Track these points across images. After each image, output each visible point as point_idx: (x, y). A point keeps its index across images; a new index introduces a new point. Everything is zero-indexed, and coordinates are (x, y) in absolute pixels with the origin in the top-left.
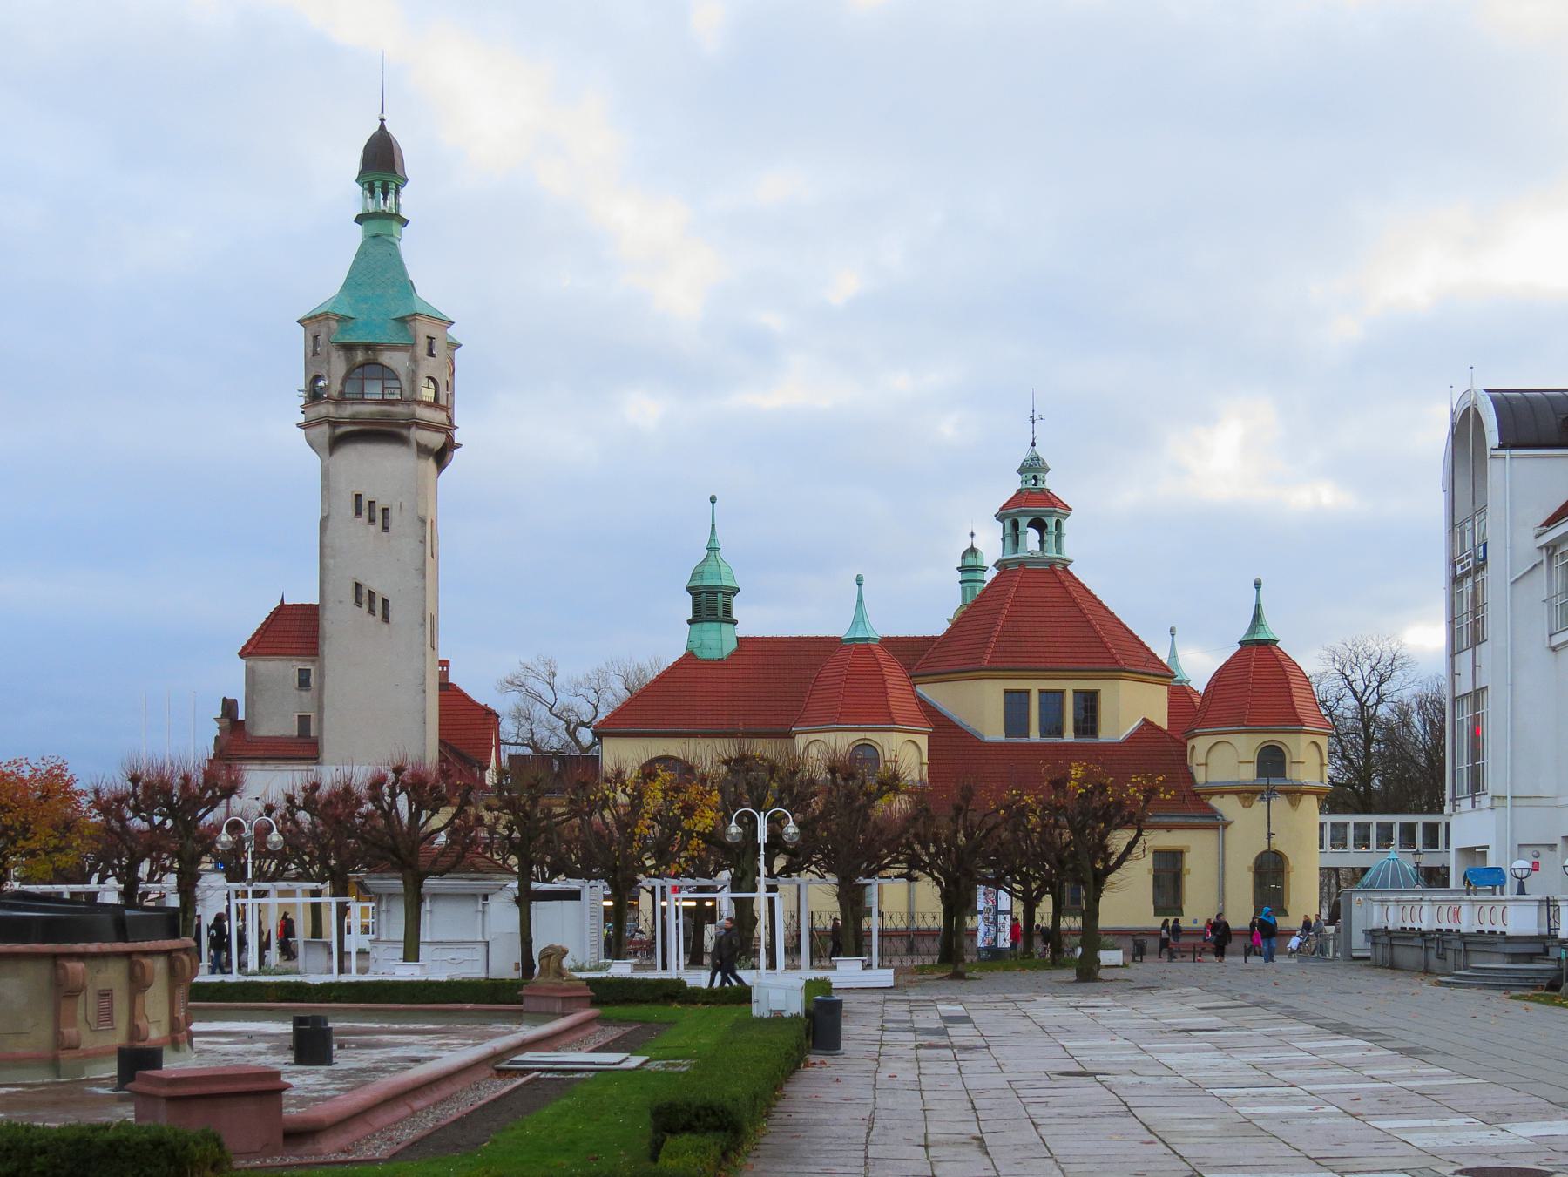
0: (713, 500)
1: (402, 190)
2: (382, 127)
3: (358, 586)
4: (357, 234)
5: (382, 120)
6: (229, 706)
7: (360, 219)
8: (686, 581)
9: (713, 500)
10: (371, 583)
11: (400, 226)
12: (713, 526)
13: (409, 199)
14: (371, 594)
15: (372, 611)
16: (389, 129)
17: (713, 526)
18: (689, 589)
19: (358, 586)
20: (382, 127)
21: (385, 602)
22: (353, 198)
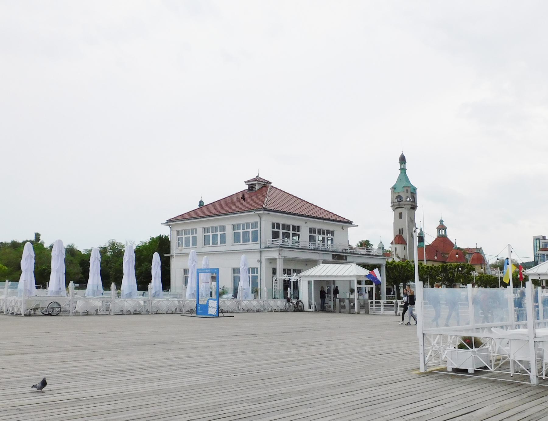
13: (407, 166)
20: (402, 153)
22: (398, 166)
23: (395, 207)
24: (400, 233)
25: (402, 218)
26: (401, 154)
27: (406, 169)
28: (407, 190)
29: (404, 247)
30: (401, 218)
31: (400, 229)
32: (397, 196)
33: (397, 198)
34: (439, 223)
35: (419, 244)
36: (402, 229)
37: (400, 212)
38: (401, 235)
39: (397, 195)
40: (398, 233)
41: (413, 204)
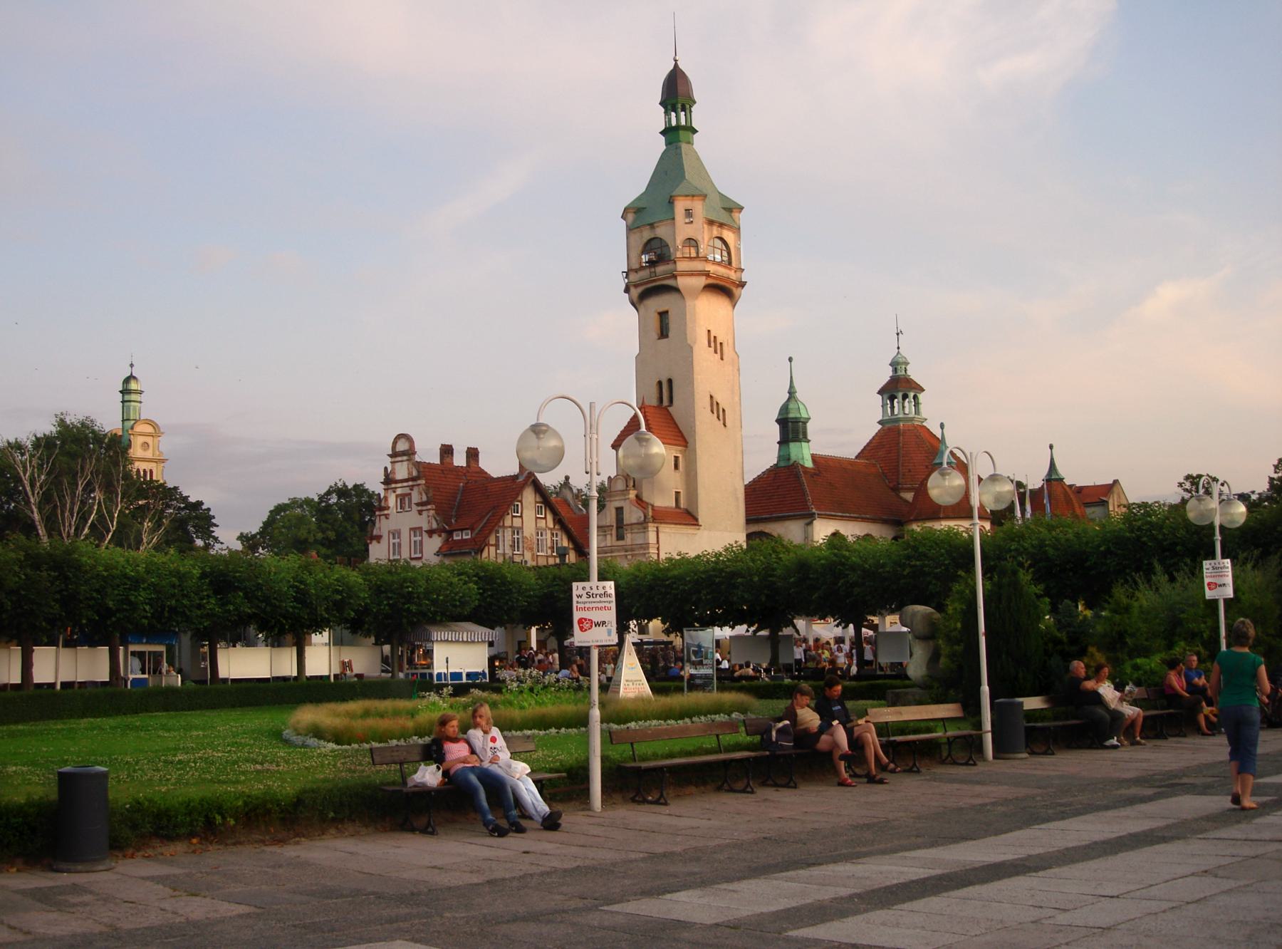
0: (790, 360)
1: (692, 109)
2: (676, 66)
3: (711, 397)
4: (659, 145)
5: (676, 61)
6: (386, 469)
7: (663, 133)
8: (775, 416)
9: (790, 360)
10: (718, 398)
11: (690, 134)
12: (791, 377)
13: (699, 116)
14: (717, 403)
15: (718, 417)
16: (681, 66)
17: (791, 377)
18: (777, 421)
19: (711, 397)
20: (676, 66)
21: (724, 410)
22: (658, 119)
23: (640, 290)
24: (661, 399)
25: (670, 334)
26: (672, 68)
27: (695, 131)
28: (689, 213)
29: (676, 458)
30: (667, 336)
31: (660, 383)
32: (645, 240)
33: (647, 247)
34: (891, 368)
35: (782, 454)
36: (670, 381)
37: (661, 310)
38: (666, 408)
39: (647, 235)
40: (654, 402)
41: (722, 271)
